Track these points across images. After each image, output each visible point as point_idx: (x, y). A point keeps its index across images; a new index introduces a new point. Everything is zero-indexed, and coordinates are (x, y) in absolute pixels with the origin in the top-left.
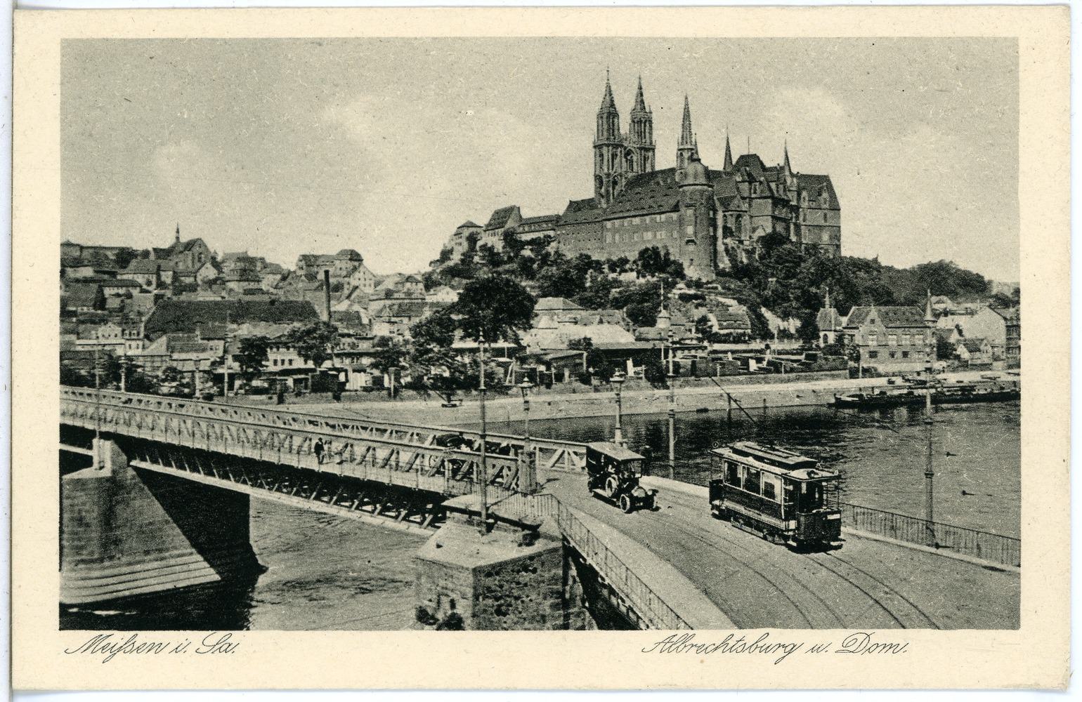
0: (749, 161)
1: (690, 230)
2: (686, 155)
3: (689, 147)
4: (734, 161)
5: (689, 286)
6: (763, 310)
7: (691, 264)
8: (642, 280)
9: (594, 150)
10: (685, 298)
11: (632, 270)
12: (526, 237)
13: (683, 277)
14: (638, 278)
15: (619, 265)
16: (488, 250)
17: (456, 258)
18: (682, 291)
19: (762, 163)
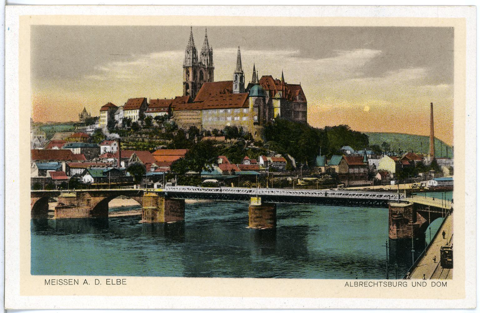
0: (267, 79)
1: (256, 118)
2: (239, 77)
3: (239, 72)
4: (260, 78)
5: (255, 145)
6: (289, 156)
7: (256, 134)
8: (228, 141)
9: (183, 68)
10: (254, 150)
11: (221, 135)
12: (154, 115)
13: (252, 140)
14: (226, 139)
15: (216, 133)
16: (127, 121)
17: (103, 123)
18: (253, 147)
19: (273, 79)
